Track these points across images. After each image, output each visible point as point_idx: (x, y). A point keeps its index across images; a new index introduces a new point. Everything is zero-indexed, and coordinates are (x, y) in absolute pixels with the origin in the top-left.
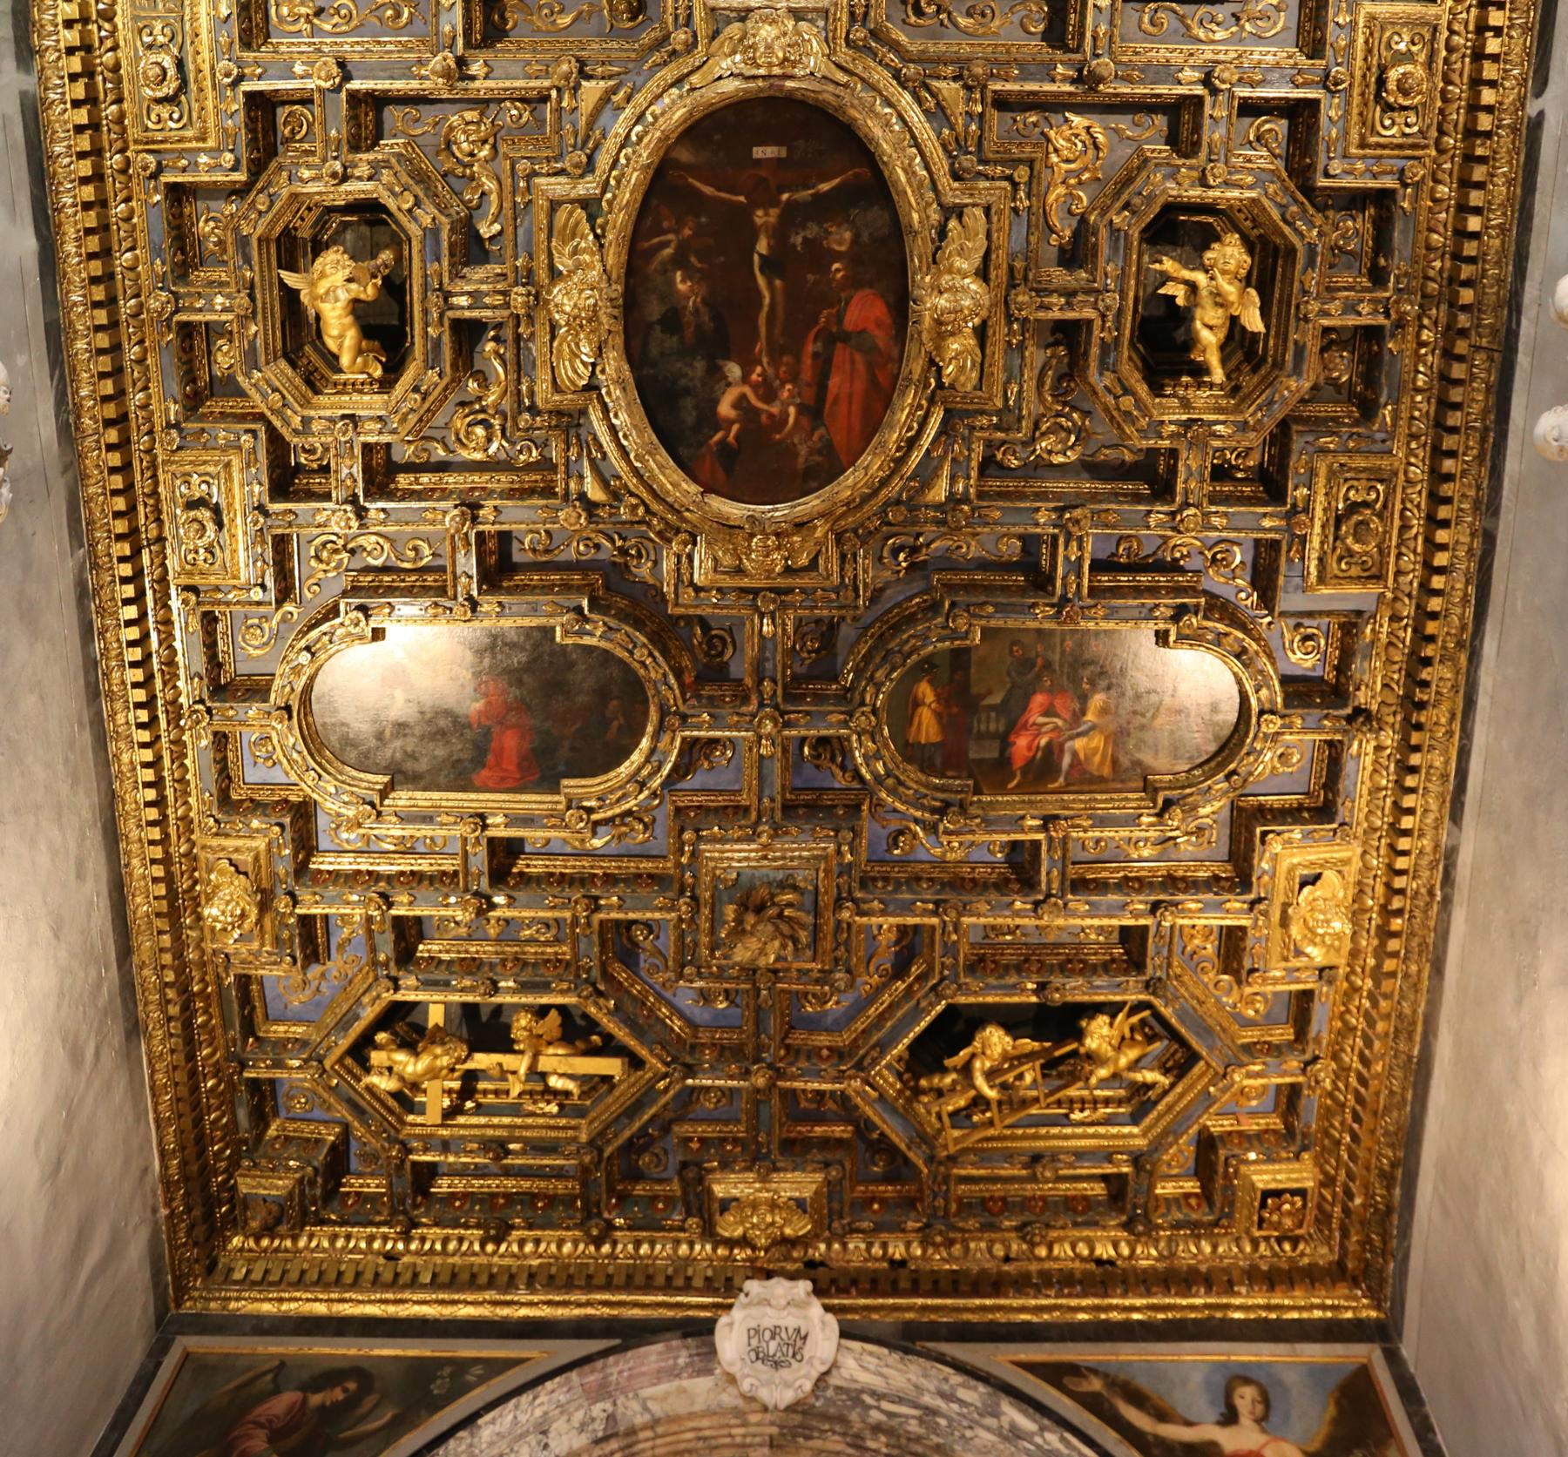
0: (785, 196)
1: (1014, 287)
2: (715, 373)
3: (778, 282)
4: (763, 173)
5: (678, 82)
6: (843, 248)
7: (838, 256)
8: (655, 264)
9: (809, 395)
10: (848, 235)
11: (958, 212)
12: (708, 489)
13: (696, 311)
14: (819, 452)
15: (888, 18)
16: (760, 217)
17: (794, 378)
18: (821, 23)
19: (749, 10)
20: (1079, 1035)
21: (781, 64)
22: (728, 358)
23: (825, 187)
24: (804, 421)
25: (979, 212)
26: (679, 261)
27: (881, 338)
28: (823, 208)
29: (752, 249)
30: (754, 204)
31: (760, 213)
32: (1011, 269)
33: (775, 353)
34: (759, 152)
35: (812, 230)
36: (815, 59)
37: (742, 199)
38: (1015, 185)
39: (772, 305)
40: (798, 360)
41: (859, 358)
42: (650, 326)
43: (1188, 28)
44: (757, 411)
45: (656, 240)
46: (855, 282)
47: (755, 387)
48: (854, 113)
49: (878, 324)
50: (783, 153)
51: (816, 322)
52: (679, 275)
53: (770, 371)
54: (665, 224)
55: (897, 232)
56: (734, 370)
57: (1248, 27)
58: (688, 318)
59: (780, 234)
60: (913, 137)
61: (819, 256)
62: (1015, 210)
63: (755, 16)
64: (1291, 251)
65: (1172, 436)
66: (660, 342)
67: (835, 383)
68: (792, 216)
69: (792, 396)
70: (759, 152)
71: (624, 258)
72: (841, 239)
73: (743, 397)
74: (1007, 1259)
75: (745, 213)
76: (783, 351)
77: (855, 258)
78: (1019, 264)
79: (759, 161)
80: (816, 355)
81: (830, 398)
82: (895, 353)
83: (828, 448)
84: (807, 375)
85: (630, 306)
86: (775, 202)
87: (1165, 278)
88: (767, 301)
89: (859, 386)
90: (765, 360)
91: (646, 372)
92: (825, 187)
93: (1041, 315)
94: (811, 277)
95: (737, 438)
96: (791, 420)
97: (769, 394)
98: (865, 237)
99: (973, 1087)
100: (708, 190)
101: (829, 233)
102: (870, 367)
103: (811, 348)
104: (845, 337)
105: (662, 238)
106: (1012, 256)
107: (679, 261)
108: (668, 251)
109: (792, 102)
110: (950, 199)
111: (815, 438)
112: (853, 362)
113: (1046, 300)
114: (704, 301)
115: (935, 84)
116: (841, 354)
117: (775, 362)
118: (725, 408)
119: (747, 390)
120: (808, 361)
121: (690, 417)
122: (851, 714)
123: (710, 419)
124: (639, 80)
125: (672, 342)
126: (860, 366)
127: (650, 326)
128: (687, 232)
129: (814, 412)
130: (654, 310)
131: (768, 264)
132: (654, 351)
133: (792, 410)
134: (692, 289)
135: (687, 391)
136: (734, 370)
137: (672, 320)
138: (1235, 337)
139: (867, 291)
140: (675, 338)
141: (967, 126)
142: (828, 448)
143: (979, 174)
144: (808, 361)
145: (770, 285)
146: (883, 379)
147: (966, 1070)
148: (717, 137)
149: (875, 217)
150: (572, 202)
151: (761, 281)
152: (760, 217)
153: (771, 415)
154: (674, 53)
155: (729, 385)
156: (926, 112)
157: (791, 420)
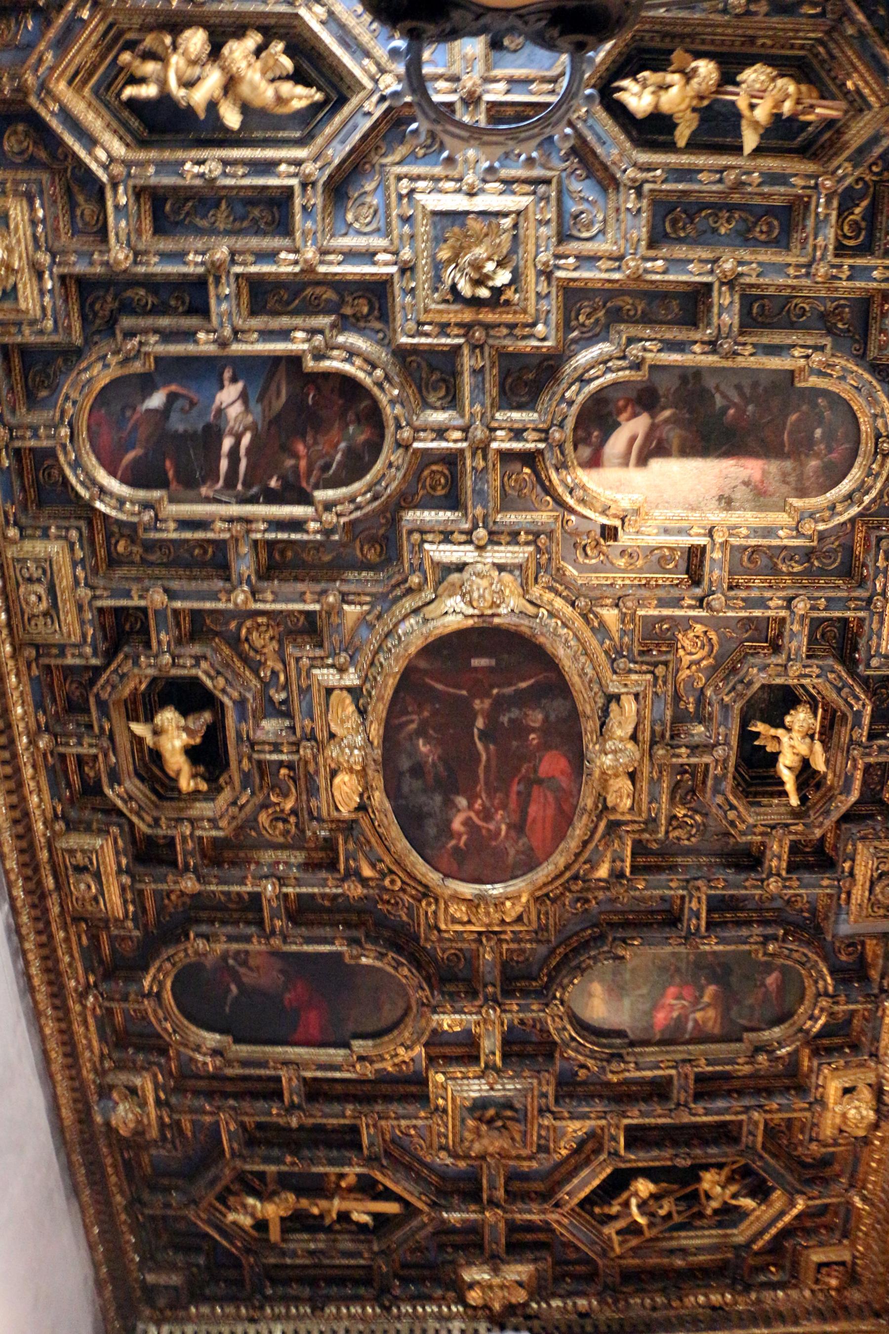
0: (495, 691)
1: (656, 743)
2: (449, 803)
3: (492, 747)
4: (480, 676)
5: (416, 611)
6: (537, 725)
7: (533, 730)
8: (403, 734)
9: (515, 818)
10: (540, 717)
11: (617, 698)
12: (446, 876)
13: (434, 764)
14: (523, 853)
15: (563, 559)
16: (477, 704)
17: (504, 806)
18: (517, 573)
19: (465, 564)
20: (699, 1180)
21: (491, 607)
22: (458, 794)
23: (523, 685)
24: (513, 834)
25: (632, 698)
26: (421, 732)
27: (564, 782)
28: (522, 699)
29: (473, 725)
30: (473, 696)
31: (477, 702)
32: (653, 732)
33: (491, 792)
34: (476, 662)
35: (515, 713)
36: (514, 602)
37: (464, 693)
38: (656, 678)
39: (488, 760)
40: (507, 796)
41: (548, 794)
42: (401, 774)
43: (776, 564)
44: (479, 828)
45: (404, 719)
46: (545, 746)
47: (477, 813)
48: (542, 639)
49: (563, 772)
50: (493, 662)
51: (519, 771)
52: (421, 742)
53: (488, 804)
54: (410, 709)
55: (574, 716)
56: (462, 802)
57: (816, 563)
58: (428, 768)
59: (492, 717)
60: (584, 649)
61: (520, 730)
62: (655, 693)
63: (469, 569)
64: (844, 716)
65: (762, 834)
66: (409, 784)
67: (533, 810)
68: (500, 704)
69: (503, 817)
70: (476, 662)
71: (381, 732)
72: (536, 718)
73: (469, 819)
74: (654, 1309)
75: (466, 703)
76: (496, 790)
77: (546, 730)
78: (658, 728)
79: (476, 669)
80: (519, 793)
81: (530, 819)
82: (575, 792)
83: (530, 851)
84: (512, 806)
85: (388, 764)
86: (488, 695)
87: (757, 735)
88: (484, 757)
89: (550, 812)
90: (484, 796)
91: (402, 802)
92: (523, 685)
93: (674, 760)
94: (515, 743)
95: (466, 844)
96: (503, 833)
97: (487, 816)
98: (552, 717)
99: (630, 1215)
100: (439, 687)
101: (526, 715)
102: (557, 800)
103: (515, 788)
104: (540, 782)
105: (409, 718)
106: (653, 722)
107: (421, 732)
108: (413, 726)
109: (498, 631)
110: (613, 689)
111: (520, 843)
112: (545, 797)
113: (678, 751)
114: (439, 758)
115: (598, 610)
116: (536, 791)
117: (489, 795)
118: (457, 825)
119: (472, 815)
120: (513, 796)
121: (432, 831)
122: (547, 1005)
123: (446, 830)
124: (386, 605)
125: (417, 784)
126: (551, 799)
127: (401, 774)
128: (426, 714)
129: (519, 827)
130: (405, 764)
131: (483, 735)
132: (405, 789)
133: (504, 827)
134: (431, 751)
135: (430, 815)
136: (462, 802)
137: (417, 770)
138: (805, 771)
139: (554, 752)
140: (420, 782)
141: (621, 638)
142: (530, 851)
143: (630, 671)
144: (513, 796)
145: (487, 749)
146: (566, 807)
147: (626, 1204)
148: (445, 652)
149: (558, 707)
150: (341, 689)
151: (480, 746)
152: (477, 704)
153: (489, 830)
154: (410, 591)
155: (459, 811)
156: (593, 629)
157: (503, 833)
